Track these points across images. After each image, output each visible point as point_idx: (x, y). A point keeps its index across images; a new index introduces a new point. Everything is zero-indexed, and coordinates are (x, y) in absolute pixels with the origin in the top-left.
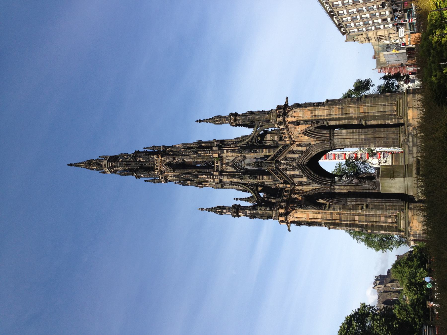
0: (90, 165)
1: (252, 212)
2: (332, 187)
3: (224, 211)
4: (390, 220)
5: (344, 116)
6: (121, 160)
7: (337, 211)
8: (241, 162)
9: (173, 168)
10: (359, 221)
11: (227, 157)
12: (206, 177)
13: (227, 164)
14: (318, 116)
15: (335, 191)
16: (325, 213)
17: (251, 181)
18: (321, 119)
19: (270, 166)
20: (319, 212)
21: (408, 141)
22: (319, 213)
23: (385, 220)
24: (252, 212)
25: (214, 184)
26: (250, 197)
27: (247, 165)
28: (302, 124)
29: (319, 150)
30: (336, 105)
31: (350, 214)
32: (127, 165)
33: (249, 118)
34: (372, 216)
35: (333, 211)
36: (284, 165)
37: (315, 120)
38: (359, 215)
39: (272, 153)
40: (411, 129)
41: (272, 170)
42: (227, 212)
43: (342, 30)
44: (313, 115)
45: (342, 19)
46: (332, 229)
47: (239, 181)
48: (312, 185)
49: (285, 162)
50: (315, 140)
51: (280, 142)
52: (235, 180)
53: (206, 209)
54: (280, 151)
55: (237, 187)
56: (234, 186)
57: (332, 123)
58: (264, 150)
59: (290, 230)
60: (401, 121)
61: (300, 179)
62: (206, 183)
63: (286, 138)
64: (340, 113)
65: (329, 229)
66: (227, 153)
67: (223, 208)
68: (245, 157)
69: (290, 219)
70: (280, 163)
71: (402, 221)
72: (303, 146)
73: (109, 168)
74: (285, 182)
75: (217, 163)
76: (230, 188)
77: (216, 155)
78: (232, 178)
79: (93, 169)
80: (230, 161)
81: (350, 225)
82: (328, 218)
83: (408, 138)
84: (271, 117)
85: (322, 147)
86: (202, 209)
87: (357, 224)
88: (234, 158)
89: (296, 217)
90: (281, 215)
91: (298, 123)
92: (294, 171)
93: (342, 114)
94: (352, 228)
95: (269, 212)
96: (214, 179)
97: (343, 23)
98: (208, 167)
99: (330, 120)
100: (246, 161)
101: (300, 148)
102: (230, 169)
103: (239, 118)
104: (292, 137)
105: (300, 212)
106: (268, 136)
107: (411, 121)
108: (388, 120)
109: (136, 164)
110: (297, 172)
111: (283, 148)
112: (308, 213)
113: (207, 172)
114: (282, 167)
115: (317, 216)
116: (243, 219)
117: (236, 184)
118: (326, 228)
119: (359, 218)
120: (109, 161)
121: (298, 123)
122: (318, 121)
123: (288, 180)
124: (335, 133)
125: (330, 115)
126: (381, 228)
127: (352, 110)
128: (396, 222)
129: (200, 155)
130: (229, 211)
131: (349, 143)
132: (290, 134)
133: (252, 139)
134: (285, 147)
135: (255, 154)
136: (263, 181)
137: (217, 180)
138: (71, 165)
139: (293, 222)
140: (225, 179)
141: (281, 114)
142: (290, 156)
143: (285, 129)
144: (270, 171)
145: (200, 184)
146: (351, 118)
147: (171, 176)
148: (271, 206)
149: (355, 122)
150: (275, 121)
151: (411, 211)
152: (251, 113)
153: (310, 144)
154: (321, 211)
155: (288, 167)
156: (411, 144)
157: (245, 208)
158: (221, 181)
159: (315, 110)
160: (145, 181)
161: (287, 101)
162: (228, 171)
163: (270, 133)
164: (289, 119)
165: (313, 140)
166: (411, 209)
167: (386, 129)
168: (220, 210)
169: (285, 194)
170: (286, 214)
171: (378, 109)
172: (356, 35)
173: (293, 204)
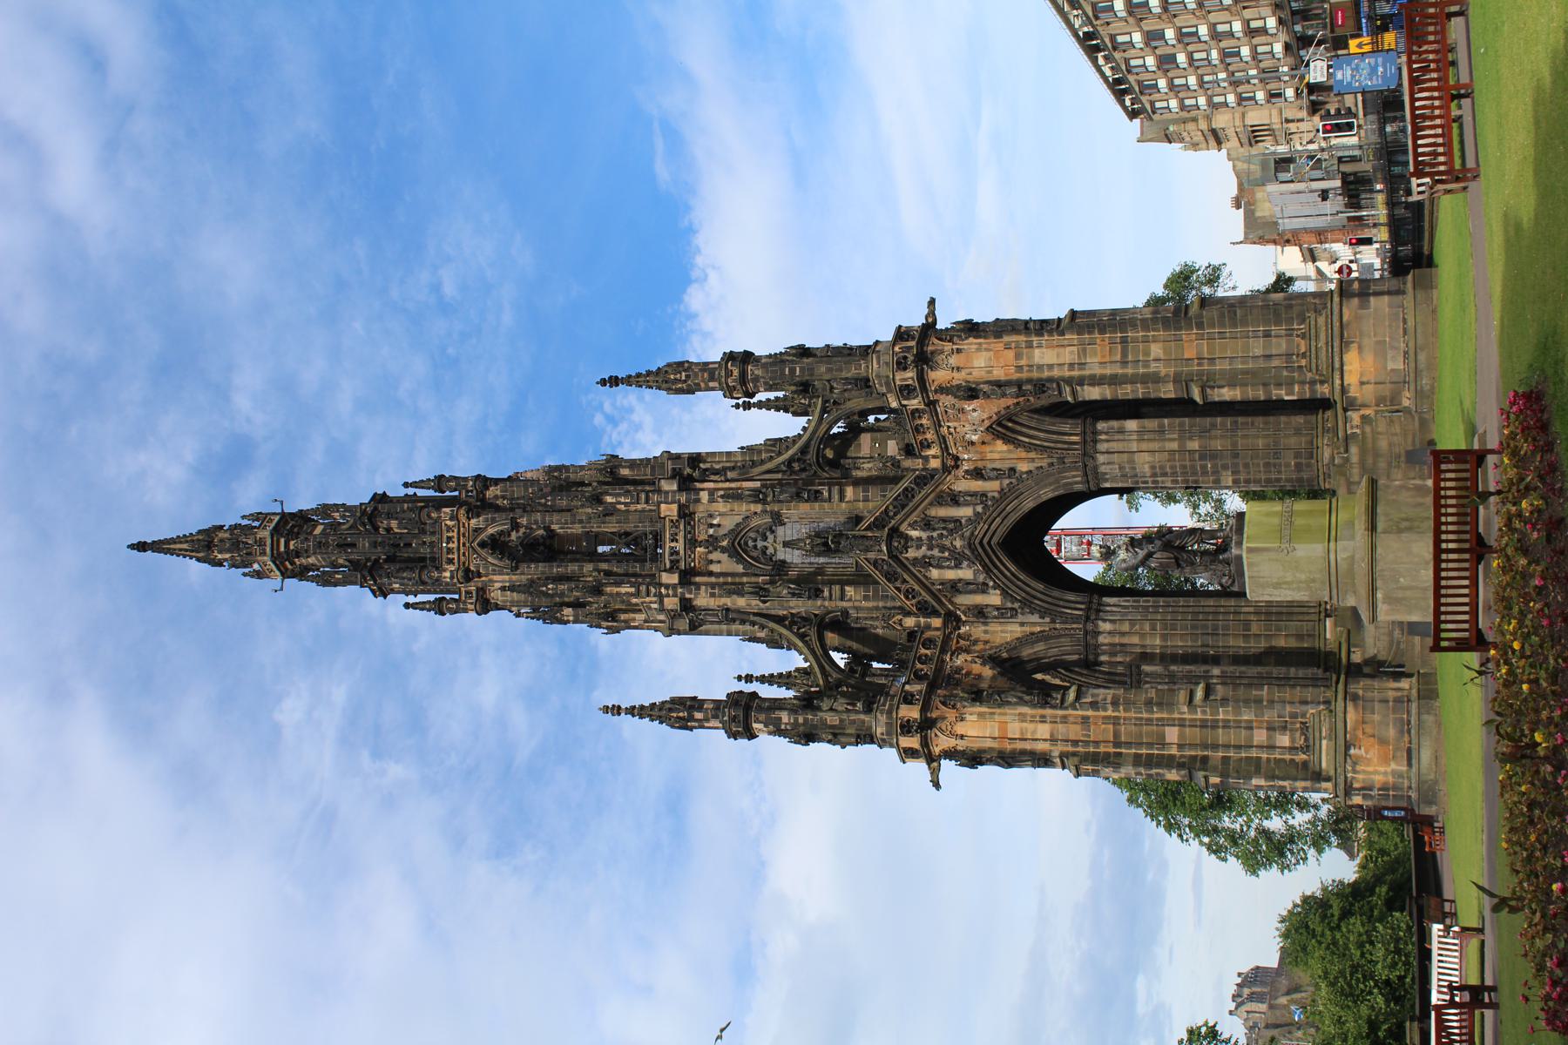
0: (209, 546)
1: (801, 720)
3: (699, 715)
4: (1284, 740)
5: (1130, 371)
6: (319, 529)
7: (1105, 710)
8: (765, 538)
9: (512, 557)
10: (1180, 746)
11: (711, 516)
12: (632, 590)
13: (712, 543)
14: (1040, 367)
15: (1101, 639)
16: (1064, 720)
17: (800, 606)
18: (1051, 380)
19: (867, 550)
20: (1043, 716)
21: (1347, 460)
22: (1043, 720)
23: (1269, 738)
24: (801, 720)
25: (662, 617)
26: (797, 670)
27: (786, 544)
28: (987, 396)
29: (1047, 493)
30: (1102, 332)
32: (343, 546)
33: (792, 371)
35: (1090, 713)
36: (919, 547)
37: (1029, 381)
38: (1182, 724)
39: (872, 504)
41: (875, 563)
42: (707, 720)
43: (1128, 103)
45: (1127, 61)
46: (1087, 775)
47: (755, 604)
48: (1020, 618)
49: (924, 535)
50: (1032, 455)
51: (907, 463)
52: (741, 602)
53: (631, 711)
54: (908, 494)
55: (748, 627)
56: (736, 627)
57: (1093, 393)
58: (849, 491)
59: (937, 785)
60: (1323, 390)
61: (979, 599)
63: (929, 447)
64: (1118, 357)
65: (1078, 775)
66: (712, 501)
67: (693, 704)
68: (778, 519)
69: (942, 742)
70: (907, 538)
71: (1324, 742)
72: (990, 479)
73: (278, 559)
74: (925, 610)
76: (721, 634)
77: (669, 510)
78: (730, 593)
79: (220, 564)
80: (722, 532)
81: (1150, 762)
82: (1072, 737)
83: (1347, 451)
84: (874, 368)
85: (1057, 481)
87: (1172, 756)
88: (739, 519)
89: (962, 737)
90: (906, 728)
92: (958, 566)
93: (1124, 363)
94: (1154, 771)
95: (862, 717)
96: (661, 597)
97: (1131, 78)
98: (641, 551)
99: (1081, 381)
100: (780, 530)
102: (723, 563)
103: (759, 372)
104: (950, 442)
105: (974, 718)
106: (865, 439)
107: (1354, 392)
108: (1279, 385)
109: (375, 545)
110: (966, 573)
111: (917, 484)
112: (1003, 718)
113: (635, 575)
114: (912, 553)
115: (1034, 732)
116: (769, 746)
117: (742, 617)
118: (1067, 774)
119: (1181, 736)
120: (276, 531)
121: (971, 389)
122: (1040, 386)
123: (935, 601)
124: (1101, 433)
126: (1256, 767)
127: (1156, 350)
128: (1306, 749)
129: (610, 512)
130: (715, 717)
131: (1147, 469)
132: (944, 430)
133: (804, 450)
134: (925, 479)
135: (817, 505)
136: (844, 604)
137: (671, 603)
138: (141, 547)
140: (703, 600)
141: (911, 358)
142: (943, 512)
143: (923, 411)
144: (869, 569)
145: (612, 619)
146: (1156, 379)
147: (503, 589)
148: (867, 693)
149: (1168, 391)
150: (888, 384)
151: (1356, 707)
152: (803, 352)
153: (1013, 470)
154: (1048, 712)
155: (936, 552)
157: (777, 704)
158: (687, 606)
159: (1030, 345)
160: (407, 606)
161: (932, 313)
162: (715, 568)
163: (871, 429)
164: (938, 376)
165: (1024, 455)
166: (1355, 698)
167: (1271, 419)
168: (681, 712)
169: (923, 651)
170: (926, 725)
171: (1246, 348)
172: (1175, 122)
173: (945, 687)
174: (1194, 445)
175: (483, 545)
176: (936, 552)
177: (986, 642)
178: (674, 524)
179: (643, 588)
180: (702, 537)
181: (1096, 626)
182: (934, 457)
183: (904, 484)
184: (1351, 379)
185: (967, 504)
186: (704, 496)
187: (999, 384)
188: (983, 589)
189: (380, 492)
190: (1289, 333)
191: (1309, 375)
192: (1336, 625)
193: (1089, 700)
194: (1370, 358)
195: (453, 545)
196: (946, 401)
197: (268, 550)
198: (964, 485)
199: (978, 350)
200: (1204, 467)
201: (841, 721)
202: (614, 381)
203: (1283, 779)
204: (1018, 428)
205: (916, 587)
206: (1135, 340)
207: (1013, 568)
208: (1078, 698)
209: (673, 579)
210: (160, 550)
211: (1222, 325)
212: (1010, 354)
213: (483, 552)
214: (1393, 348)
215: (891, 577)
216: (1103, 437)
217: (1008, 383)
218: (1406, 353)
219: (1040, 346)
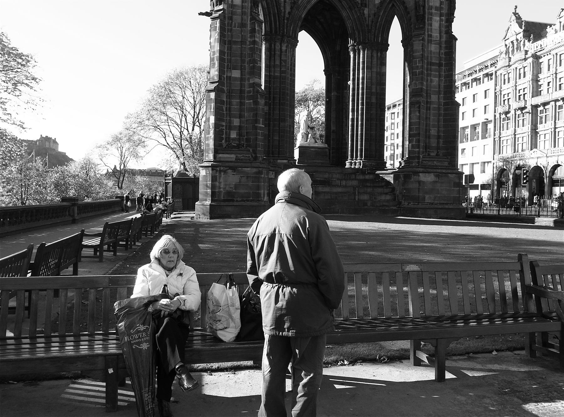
4: (234, 135)
7: (251, 37)
10: (229, 78)
15: (278, 44)
16: (243, 13)
18: (425, 25)
30: (446, 54)
31: (243, 61)
34: (240, 102)
38: (242, 79)
44: (433, 11)
64: (433, 61)
71: (233, 156)
82: (235, 17)
83: (369, 173)
93: (432, 64)
119: (236, 79)
159: (441, 15)
190: (438, 148)
212: (438, 4)
216: (379, 54)
218: (432, 204)
219: (441, 20)
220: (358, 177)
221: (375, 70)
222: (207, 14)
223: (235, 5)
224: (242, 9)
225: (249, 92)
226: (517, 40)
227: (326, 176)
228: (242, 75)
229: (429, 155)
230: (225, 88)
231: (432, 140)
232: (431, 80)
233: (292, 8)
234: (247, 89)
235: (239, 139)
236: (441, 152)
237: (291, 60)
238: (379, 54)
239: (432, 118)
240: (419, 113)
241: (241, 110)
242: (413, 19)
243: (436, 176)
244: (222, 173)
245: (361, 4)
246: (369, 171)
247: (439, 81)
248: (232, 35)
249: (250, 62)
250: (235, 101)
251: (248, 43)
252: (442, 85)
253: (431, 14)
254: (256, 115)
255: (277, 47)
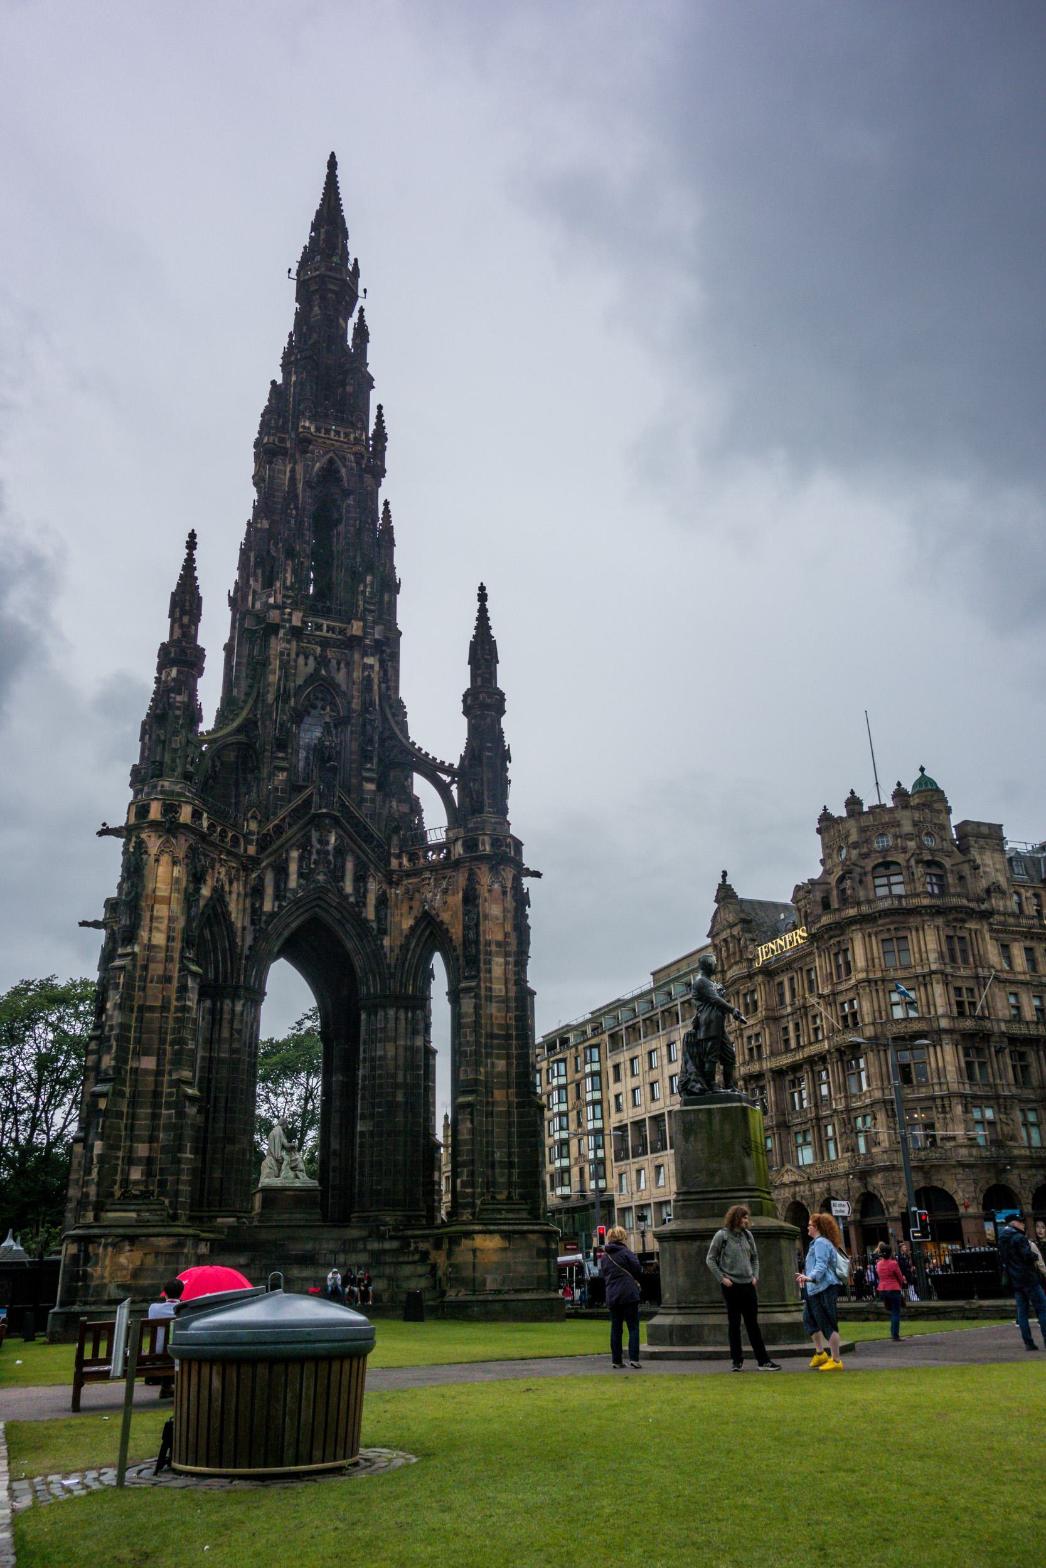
1: (178, 712)
2: (242, 992)
3: (186, 620)
4: (136, 1174)
7: (177, 999)
10: (135, 1071)
11: (348, 664)
12: (288, 583)
13: (322, 661)
14: (489, 962)
15: (228, 1003)
16: (169, 959)
18: (478, 971)
19: (320, 794)
22: (169, 939)
25: (258, 605)
28: (466, 913)
33: (489, 749)
35: (175, 984)
36: (320, 842)
37: (478, 950)
38: (159, 1073)
40: (424, 1246)
42: (182, 626)
44: (494, 948)
49: (330, 847)
50: (397, 951)
54: (369, 838)
61: (269, 890)
62: (260, 580)
63: (410, 860)
64: (496, 1031)
66: (366, 667)
69: (153, 843)
71: (134, 1215)
75: (328, 626)
77: (356, 628)
81: (122, 1039)
82: (152, 966)
83: (392, 1238)
86: (191, 544)
87: (126, 1062)
88: (344, 688)
89: (157, 860)
90: (170, 809)
91: (470, 899)
92: (301, 875)
93: (492, 1036)
95: (179, 770)
99: (477, 996)
101: (371, 900)
102: (305, 668)
107: (465, 1243)
108: (472, 1174)
110: (293, 883)
114: (315, 835)
115: (158, 930)
119: (146, 1072)
125: (489, 998)
131: (380, 1053)
132: (427, 875)
136: (265, 772)
137: (274, 616)
138: (332, 164)
139: (141, 846)
140: (277, 645)
142: (350, 866)
151: (173, 1246)
154: (177, 945)
156: (374, 1246)
158: (273, 629)
159: (506, 955)
168: (186, 603)
170: (169, 827)
174: (400, 1098)
175: (331, 461)
176: (314, 857)
177: (230, 892)
178: (342, 632)
179: (290, 593)
180: (329, 654)
181: (239, 998)
182: (401, 864)
183: (377, 834)
184: (480, 1242)
185: (356, 890)
186: (369, 660)
187: (477, 925)
188: (278, 896)
189: (374, 384)
191: (478, 1202)
192: (229, 1227)
193: (190, 984)
194: (495, 1258)
195: (332, 434)
196: (461, 879)
197: (330, 273)
198: (372, 886)
199: (505, 910)
200: (380, 1105)
201: (175, 750)
202: (483, 597)
203: (99, 1173)
204: (423, 939)
205: (284, 836)
206: (508, 1047)
207: (294, 925)
208: (194, 974)
209: (296, 621)
210: (328, 176)
211: (520, 1124)
213: (325, 460)
214: (504, 1280)
215: (297, 814)
216: (410, 1015)
217: (478, 933)
218: (499, 1292)
219: (507, 963)
220: (369, 1247)
221: (401, 1043)
222: (96, 925)
223: (154, 946)
224: (167, 951)
225: (170, 1095)
226: (733, 936)
227: (309, 1246)
228: (158, 1065)
229: (493, 1198)
230: (127, 1090)
231: (498, 1171)
232: (493, 1063)
233: (255, 939)
234: (166, 1090)
235: (146, 1181)
236: (516, 1193)
237: (252, 1026)
238: (410, 1015)
239: (496, 1130)
240: (472, 1122)
241: (154, 1128)
242: (462, 961)
243: (502, 1238)
244: (110, 1249)
245: (379, 929)
246: (392, 1233)
247: (509, 1065)
248: (145, 997)
249: (172, 1044)
250: (144, 1111)
251: (172, 1009)
252: (514, 1070)
253: (490, 953)
254: (180, 1137)
255: (225, 1007)
